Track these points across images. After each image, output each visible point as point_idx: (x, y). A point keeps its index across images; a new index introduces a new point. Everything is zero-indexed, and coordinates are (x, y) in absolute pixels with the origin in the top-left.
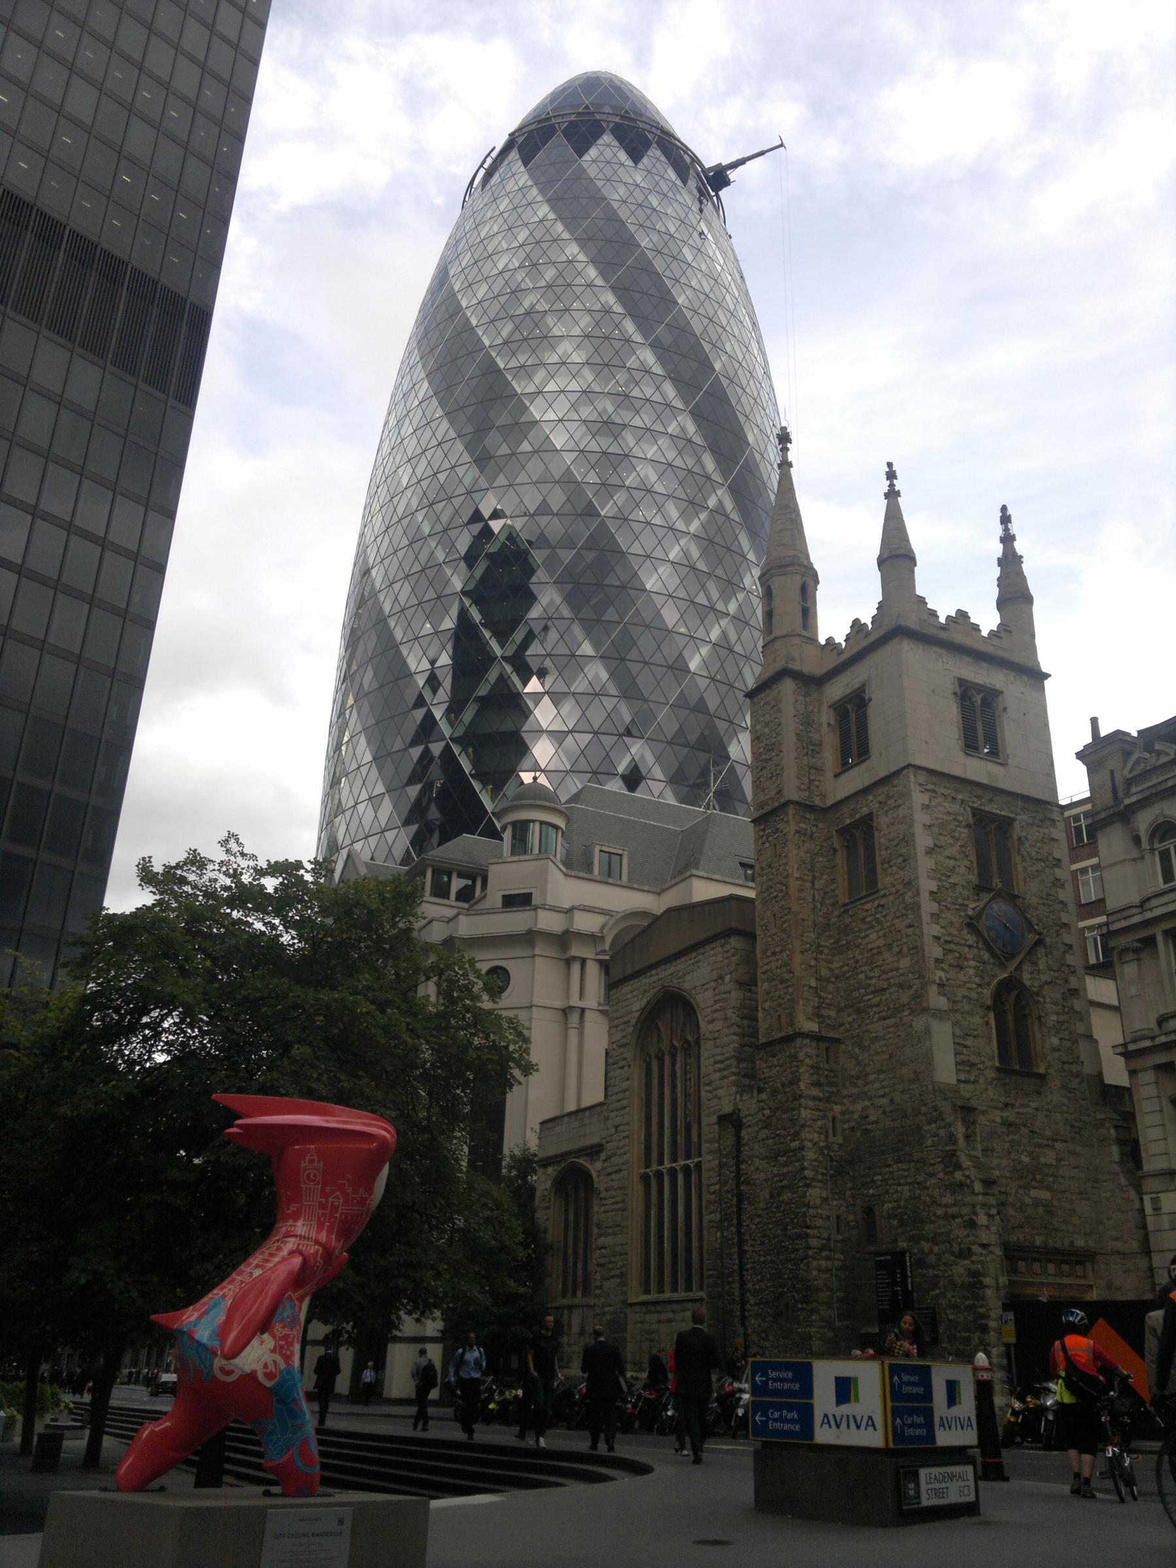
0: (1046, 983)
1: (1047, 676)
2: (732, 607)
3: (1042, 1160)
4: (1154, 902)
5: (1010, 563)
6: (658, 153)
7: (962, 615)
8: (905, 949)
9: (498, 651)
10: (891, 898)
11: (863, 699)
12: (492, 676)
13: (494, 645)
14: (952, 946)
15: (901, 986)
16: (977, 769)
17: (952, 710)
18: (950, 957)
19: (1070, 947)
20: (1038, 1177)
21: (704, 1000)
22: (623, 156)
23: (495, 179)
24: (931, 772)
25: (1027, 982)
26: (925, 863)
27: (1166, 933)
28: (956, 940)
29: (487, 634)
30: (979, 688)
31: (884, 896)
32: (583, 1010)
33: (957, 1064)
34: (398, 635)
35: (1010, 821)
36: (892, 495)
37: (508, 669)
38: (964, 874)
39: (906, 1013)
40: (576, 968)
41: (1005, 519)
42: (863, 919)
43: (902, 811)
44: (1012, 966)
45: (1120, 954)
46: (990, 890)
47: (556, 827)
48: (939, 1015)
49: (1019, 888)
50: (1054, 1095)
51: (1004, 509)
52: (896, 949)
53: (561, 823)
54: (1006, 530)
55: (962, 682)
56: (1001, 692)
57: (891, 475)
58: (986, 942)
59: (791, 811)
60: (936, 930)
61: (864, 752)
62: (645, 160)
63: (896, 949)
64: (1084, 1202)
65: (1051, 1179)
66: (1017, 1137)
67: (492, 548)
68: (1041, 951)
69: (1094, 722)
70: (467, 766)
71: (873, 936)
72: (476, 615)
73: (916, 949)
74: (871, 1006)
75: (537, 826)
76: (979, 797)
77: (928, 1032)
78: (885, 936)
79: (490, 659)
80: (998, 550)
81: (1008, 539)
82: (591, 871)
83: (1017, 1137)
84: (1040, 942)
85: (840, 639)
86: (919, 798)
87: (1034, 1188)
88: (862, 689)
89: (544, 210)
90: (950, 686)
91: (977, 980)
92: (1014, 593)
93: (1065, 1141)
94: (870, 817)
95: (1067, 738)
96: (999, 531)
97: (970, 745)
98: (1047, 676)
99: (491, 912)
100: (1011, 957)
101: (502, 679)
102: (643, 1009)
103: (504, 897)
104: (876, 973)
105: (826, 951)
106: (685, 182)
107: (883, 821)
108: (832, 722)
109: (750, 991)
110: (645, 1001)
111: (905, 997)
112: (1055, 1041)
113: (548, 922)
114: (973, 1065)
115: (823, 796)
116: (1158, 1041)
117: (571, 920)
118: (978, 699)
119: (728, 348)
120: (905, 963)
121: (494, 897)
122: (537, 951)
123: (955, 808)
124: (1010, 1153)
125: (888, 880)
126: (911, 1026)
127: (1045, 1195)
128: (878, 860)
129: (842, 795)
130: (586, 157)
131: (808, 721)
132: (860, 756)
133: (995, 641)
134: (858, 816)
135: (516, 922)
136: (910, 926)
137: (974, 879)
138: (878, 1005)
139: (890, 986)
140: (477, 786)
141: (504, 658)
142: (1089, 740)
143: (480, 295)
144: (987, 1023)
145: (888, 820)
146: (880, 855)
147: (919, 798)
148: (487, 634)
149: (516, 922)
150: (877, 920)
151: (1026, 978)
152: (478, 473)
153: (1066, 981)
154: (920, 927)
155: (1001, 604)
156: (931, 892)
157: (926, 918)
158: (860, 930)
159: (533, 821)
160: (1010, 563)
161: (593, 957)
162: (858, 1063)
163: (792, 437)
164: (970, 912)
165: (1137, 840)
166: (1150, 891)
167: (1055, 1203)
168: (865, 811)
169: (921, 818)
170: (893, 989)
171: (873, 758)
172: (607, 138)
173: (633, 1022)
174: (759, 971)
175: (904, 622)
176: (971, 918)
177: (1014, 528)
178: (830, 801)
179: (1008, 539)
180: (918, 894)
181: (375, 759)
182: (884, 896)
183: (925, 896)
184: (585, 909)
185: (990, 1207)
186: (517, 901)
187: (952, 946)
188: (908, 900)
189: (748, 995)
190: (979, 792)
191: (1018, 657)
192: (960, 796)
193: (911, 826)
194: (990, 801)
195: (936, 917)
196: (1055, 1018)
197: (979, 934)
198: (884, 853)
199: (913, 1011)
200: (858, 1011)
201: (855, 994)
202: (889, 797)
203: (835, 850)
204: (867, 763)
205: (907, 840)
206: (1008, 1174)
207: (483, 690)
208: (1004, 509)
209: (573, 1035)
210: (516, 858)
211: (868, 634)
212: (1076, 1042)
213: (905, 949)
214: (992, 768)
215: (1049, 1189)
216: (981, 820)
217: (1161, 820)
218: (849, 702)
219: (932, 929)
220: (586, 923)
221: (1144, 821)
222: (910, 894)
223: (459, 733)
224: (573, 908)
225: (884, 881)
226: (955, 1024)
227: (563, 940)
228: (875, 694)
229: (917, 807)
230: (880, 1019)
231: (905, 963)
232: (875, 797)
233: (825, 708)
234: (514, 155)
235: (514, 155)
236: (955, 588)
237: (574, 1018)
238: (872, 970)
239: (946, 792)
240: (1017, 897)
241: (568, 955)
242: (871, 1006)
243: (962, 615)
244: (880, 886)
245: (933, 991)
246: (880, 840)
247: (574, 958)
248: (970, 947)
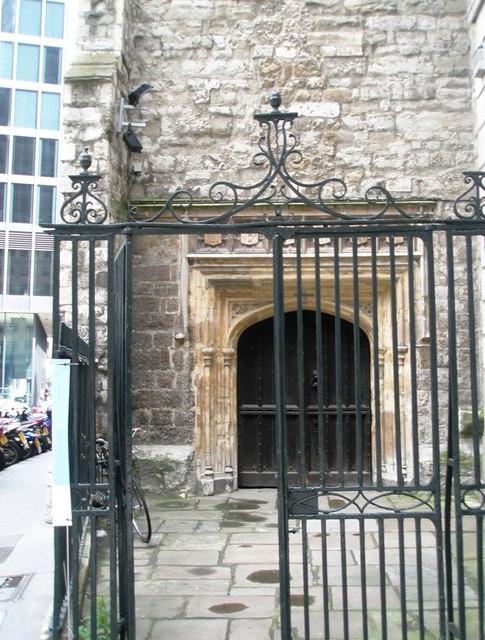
3: (328, 50)
20: (313, 81)
64: (425, 114)
65: (347, 81)
66: (274, 18)
83: (274, 18)
87: (300, 99)
93: (395, 12)
124: (250, 46)
127: (329, 109)
167: (348, 120)
185: (84, 127)
206: (242, 84)
215: (339, 99)
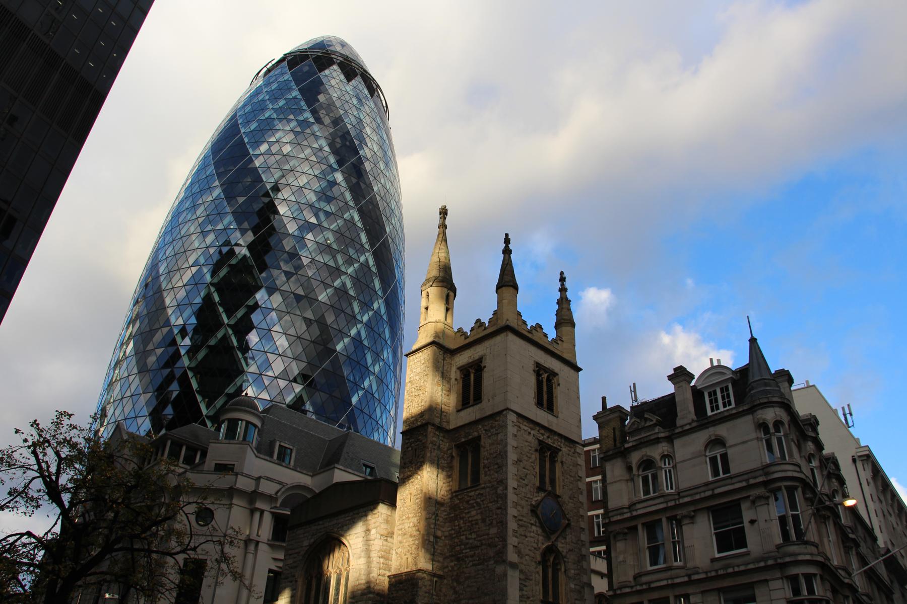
0: (570, 550)
1: (580, 369)
2: (365, 318)
4: (638, 506)
5: (564, 303)
6: (361, 80)
7: (539, 326)
8: (494, 522)
9: (226, 321)
10: (488, 490)
11: (480, 366)
12: (220, 334)
13: (224, 316)
14: (521, 523)
15: (489, 545)
16: (542, 416)
17: (532, 380)
18: (521, 529)
19: (583, 529)
22: (342, 77)
23: (271, 74)
24: (520, 415)
25: (560, 549)
26: (511, 470)
27: (643, 524)
28: (524, 519)
29: (221, 309)
30: (546, 370)
31: (484, 488)
32: (258, 543)
33: (521, 597)
34: (168, 301)
36: (507, 252)
37: (230, 332)
39: (492, 562)
40: (257, 515)
41: (562, 279)
42: (467, 502)
43: (500, 437)
44: (553, 537)
45: (615, 537)
46: (545, 491)
47: (255, 426)
48: (513, 566)
49: (559, 491)
51: (562, 273)
52: (488, 522)
53: (259, 425)
54: (563, 285)
55: (538, 365)
56: (557, 374)
57: (507, 241)
58: (540, 523)
59: (430, 428)
61: (478, 399)
62: (353, 81)
63: (488, 522)
67: (233, 261)
68: (568, 531)
69: (604, 399)
70: (195, 385)
71: (473, 513)
72: (217, 298)
73: (503, 524)
74: (467, 557)
75: (244, 423)
76: (543, 435)
77: (505, 575)
78: (481, 513)
79: (220, 324)
80: (558, 295)
81: (563, 290)
82: (271, 456)
84: (568, 525)
85: (467, 329)
88: (481, 359)
89: (295, 93)
90: (531, 367)
91: (535, 545)
92: (565, 320)
94: (479, 438)
95: (589, 407)
96: (558, 285)
97: (539, 403)
98: (580, 369)
99: (208, 472)
100: (554, 532)
101: (225, 338)
102: (310, 546)
103: (216, 464)
104: (474, 536)
105: (441, 519)
106: (372, 96)
107: (485, 442)
108: (459, 378)
109: (386, 540)
110: (312, 540)
111: (491, 553)
112: (573, 586)
113: (243, 483)
114: (528, 598)
115: (448, 422)
116: (634, 589)
117: (258, 485)
118: (545, 376)
119: (382, 181)
120: (494, 531)
121: (210, 463)
122: (234, 501)
123: (530, 438)
125: (487, 478)
126: (494, 571)
128: (482, 465)
129: (460, 423)
130: (322, 73)
132: (474, 400)
133: (555, 345)
134: (470, 437)
136: (498, 508)
137: (538, 484)
138: (472, 556)
139: (482, 544)
140: (199, 398)
141: (229, 325)
142: (600, 409)
143: (252, 128)
144: (538, 572)
145: (490, 441)
146: (484, 462)
147: (511, 430)
148: (221, 309)
149: (224, 481)
150: (477, 503)
151: (560, 546)
152: (232, 219)
153: (580, 550)
154: (506, 509)
155: (557, 327)
156: (514, 488)
157: (510, 504)
158: (465, 509)
159: (242, 420)
160: (564, 303)
161: (268, 509)
162: (456, 592)
163: (449, 213)
164: (534, 503)
165: (629, 469)
166: (635, 499)
168: (476, 434)
169: (511, 442)
170: (483, 547)
171: (484, 402)
172: (335, 67)
173: (302, 553)
174: (396, 529)
175: (504, 326)
176: (534, 506)
177: (567, 284)
178: (452, 426)
179: (563, 290)
180: (506, 488)
181: (139, 372)
182: (484, 488)
183: (510, 489)
184: (269, 479)
186: (222, 468)
187: (521, 523)
188: (499, 492)
189: (385, 543)
190: (542, 431)
191: (566, 356)
192: (532, 432)
193: (506, 446)
194: (548, 437)
195: (516, 505)
196: (573, 571)
197: (537, 516)
198: (486, 462)
199: (496, 562)
200: (458, 559)
201: (458, 548)
202: (492, 427)
203: (453, 457)
204: (479, 405)
205: (503, 455)
207: (212, 342)
208: (562, 273)
209: (250, 557)
210: (227, 441)
211: (485, 329)
212: (583, 587)
213: (494, 522)
214: (550, 417)
217: (645, 458)
218: (471, 367)
219: (512, 511)
220: (267, 488)
221: (635, 458)
222: (501, 488)
223: (193, 365)
224: (260, 478)
225: (483, 478)
226: (521, 571)
227: (253, 496)
228: (488, 363)
229: (510, 435)
230: (473, 565)
231: (494, 531)
232: (483, 426)
233: (454, 369)
234: (285, 63)
235: (285, 63)
236: (536, 309)
237: (252, 547)
238: (471, 534)
239: (526, 428)
240: (559, 497)
241: (253, 507)
242: (467, 557)
243: (539, 326)
244: (481, 482)
245: (510, 549)
246: (484, 453)
247: (257, 509)
248: (532, 524)
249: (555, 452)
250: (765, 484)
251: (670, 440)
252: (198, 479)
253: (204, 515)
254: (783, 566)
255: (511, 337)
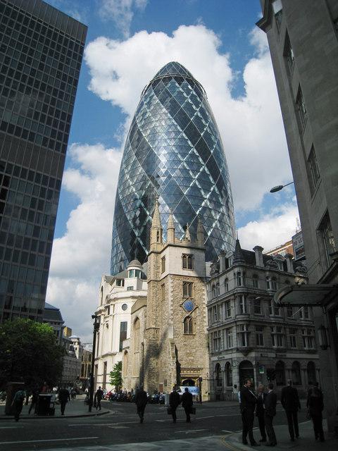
17: (181, 261)
21: (141, 319)
22: (177, 84)
35: (192, 283)
38: (181, 295)
50: (197, 338)
60: (172, 308)
72: (143, 205)
86: (170, 281)
90: (181, 255)
97: (184, 267)
131: (157, 262)
135: (131, 293)
195: (172, 305)
216: (185, 283)
249: (191, 284)
250: (234, 294)
251: (218, 277)
252: (119, 295)
253: (124, 307)
254: (236, 322)
255: (171, 247)
